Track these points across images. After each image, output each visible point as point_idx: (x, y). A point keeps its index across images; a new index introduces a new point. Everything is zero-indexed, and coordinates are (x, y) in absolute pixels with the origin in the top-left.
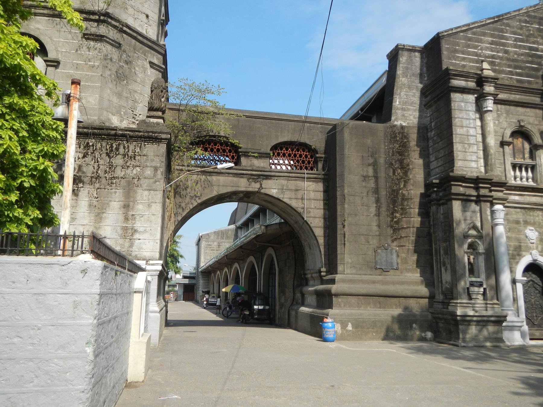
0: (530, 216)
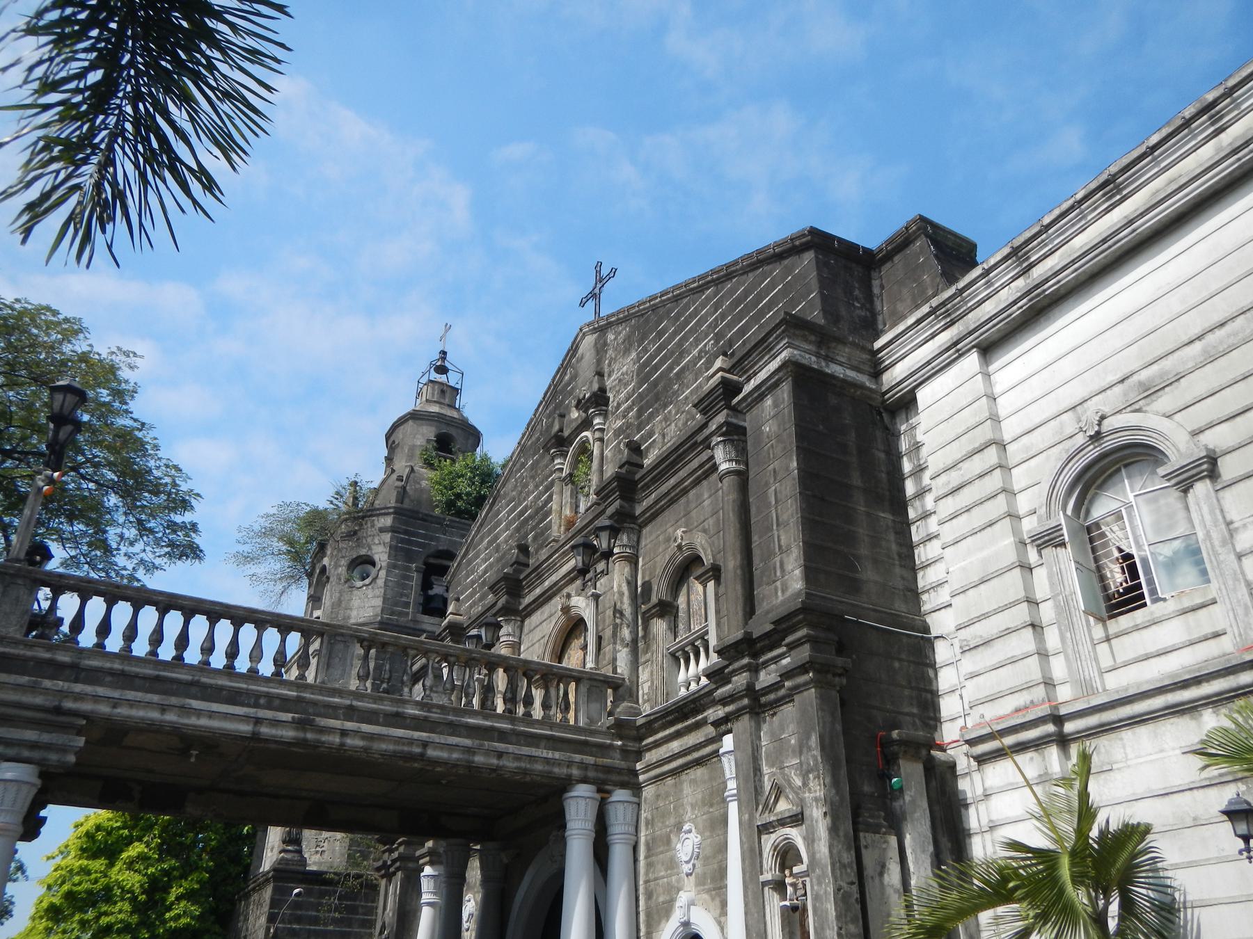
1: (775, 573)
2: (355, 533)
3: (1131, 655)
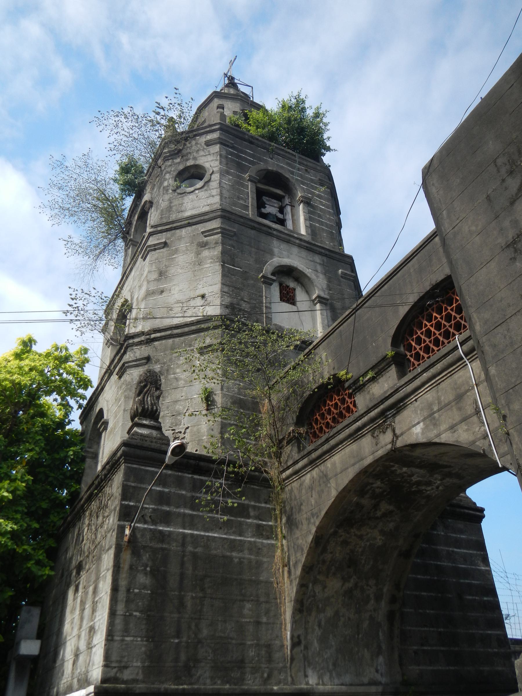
2: (180, 151)
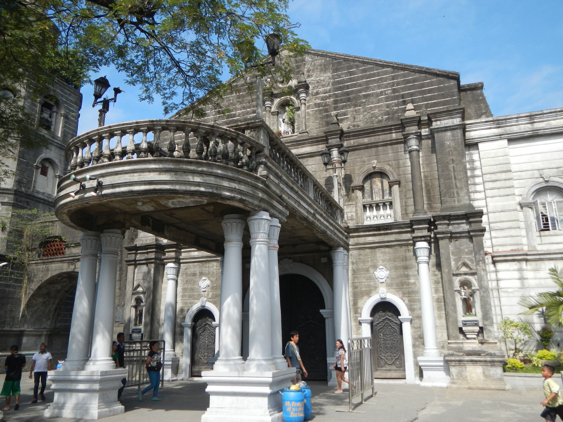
0: (206, 267)
1: (454, 195)
3: (547, 242)
